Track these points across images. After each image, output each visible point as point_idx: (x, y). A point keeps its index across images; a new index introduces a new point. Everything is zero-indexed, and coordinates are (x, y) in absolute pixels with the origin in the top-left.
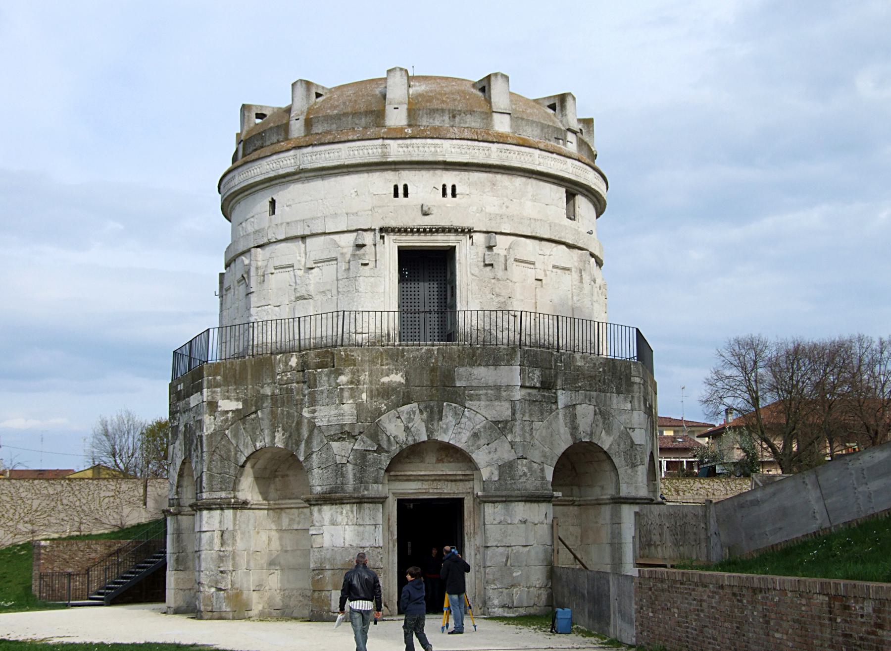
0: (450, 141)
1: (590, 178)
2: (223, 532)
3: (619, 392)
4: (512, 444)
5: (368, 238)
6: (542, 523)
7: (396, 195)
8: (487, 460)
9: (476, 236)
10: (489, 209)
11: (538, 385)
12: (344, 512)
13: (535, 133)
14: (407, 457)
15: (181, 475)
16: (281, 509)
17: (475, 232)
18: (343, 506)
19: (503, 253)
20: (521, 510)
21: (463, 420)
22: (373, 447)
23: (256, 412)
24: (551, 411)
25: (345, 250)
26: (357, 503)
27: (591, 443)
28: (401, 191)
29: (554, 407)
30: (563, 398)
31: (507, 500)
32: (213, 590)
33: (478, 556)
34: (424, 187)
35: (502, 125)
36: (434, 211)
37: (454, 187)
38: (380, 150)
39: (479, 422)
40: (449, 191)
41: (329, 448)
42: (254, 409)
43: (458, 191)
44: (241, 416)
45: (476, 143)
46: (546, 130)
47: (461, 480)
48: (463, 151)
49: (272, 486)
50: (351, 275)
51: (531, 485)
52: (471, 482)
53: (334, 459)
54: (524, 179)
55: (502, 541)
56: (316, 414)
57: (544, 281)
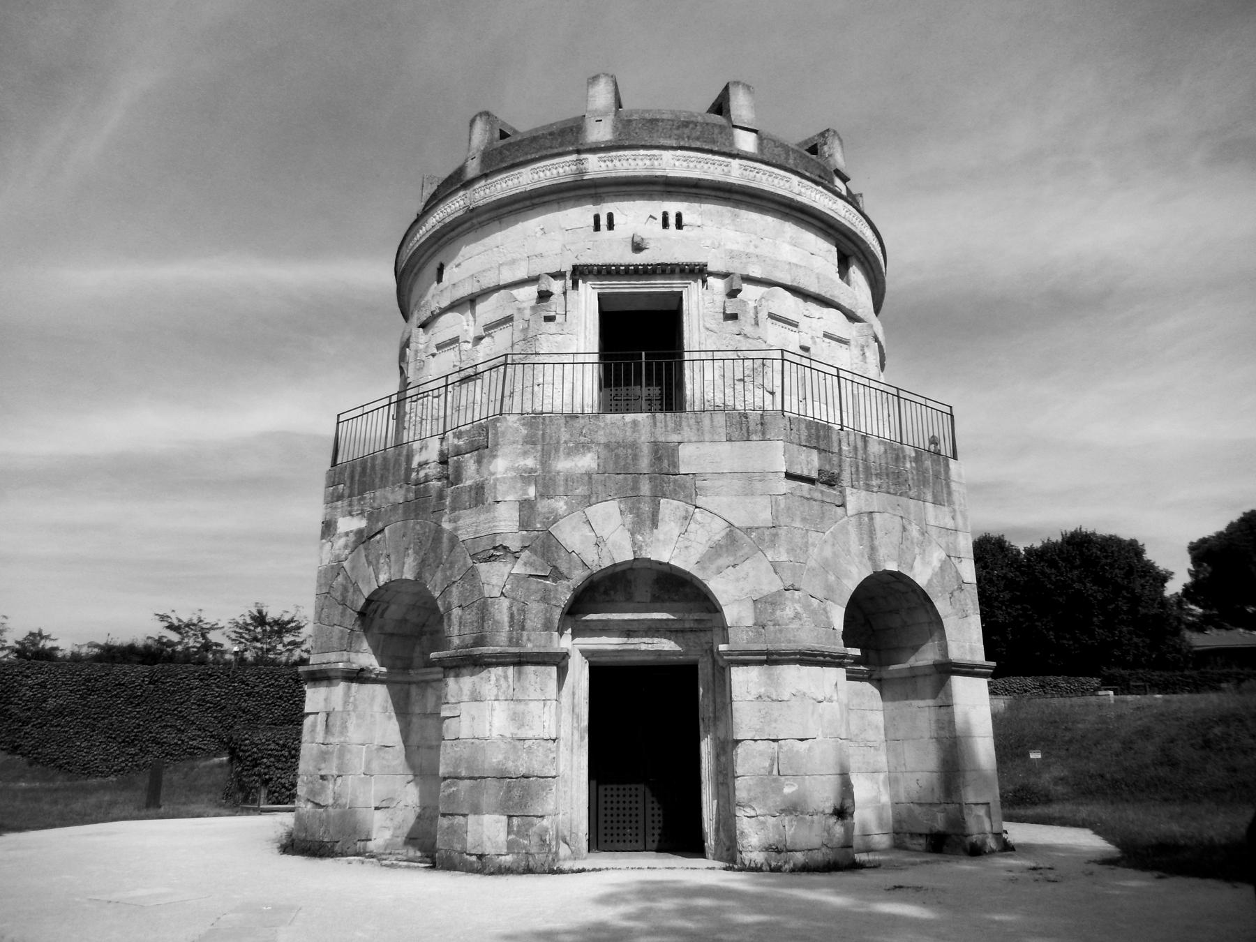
0: (671, 152)
2: (328, 715)
3: (937, 502)
4: (775, 567)
6: (830, 701)
7: (597, 227)
8: (733, 592)
9: (710, 280)
10: (730, 246)
12: (493, 678)
14: (606, 593)
16: (427, 682)
17: (711, 274)
18: (492, 670)
19: (752, 304)
20: (794, 676)
21: (693, 526)
22: (544, 570)
23: (382, 531)
25: (522, 306)
26: (514, 664)
27: (898, 577)
28: (604, 221)
30: (855, 500)
31: (771, 659)
32: (310, 806)
33: (723, 759)
34: (635, 216)
36: (651, 245)
37: (679, 216)
38: (574, 168)
39: (717, 529)
40: (672, 220)
41: (472, 574)
42: (380, 525)
43: (685, 220)
44: (363, 539)
45: (710, 156)
47: (692, 631)
48: (692, 165)
49: (418, 649)
50: (531, 334)
52: (709, 634)
53: (481, 593)
55: (762, 730)
56: (460, 523)
57: (812, 350)
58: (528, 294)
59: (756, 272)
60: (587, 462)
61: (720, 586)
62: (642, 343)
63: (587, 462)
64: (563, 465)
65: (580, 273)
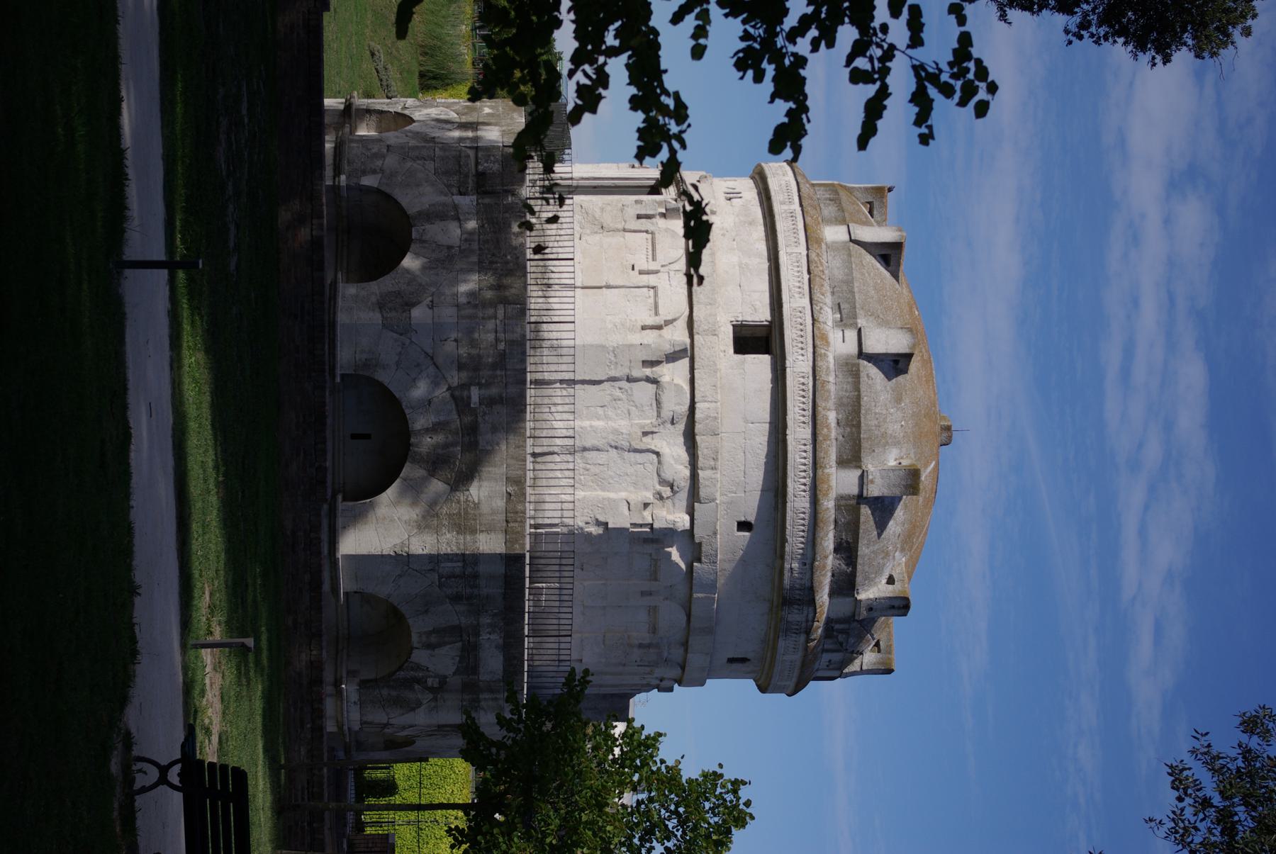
11: (480, 168)
13: (836, 272)
24: (449, 186)
29: (455, 190)
35: (834, 234)
46: (845, 288)
54: (765, 253)
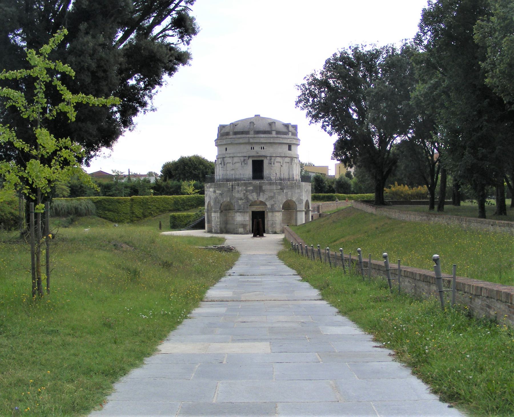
1: (294, 142)
5: (246, 158)
15: (208, 204)
30: (285, 191)
34: (257, 148)
44: (221, 194)
51: (277, 209)
58: (242, 159)
59: (274, 155)
60: (251, 188)
61: (267, 203)
62: (258, 167)
63: (251, 188)
64: (249, 188)
65: (249, 157)
